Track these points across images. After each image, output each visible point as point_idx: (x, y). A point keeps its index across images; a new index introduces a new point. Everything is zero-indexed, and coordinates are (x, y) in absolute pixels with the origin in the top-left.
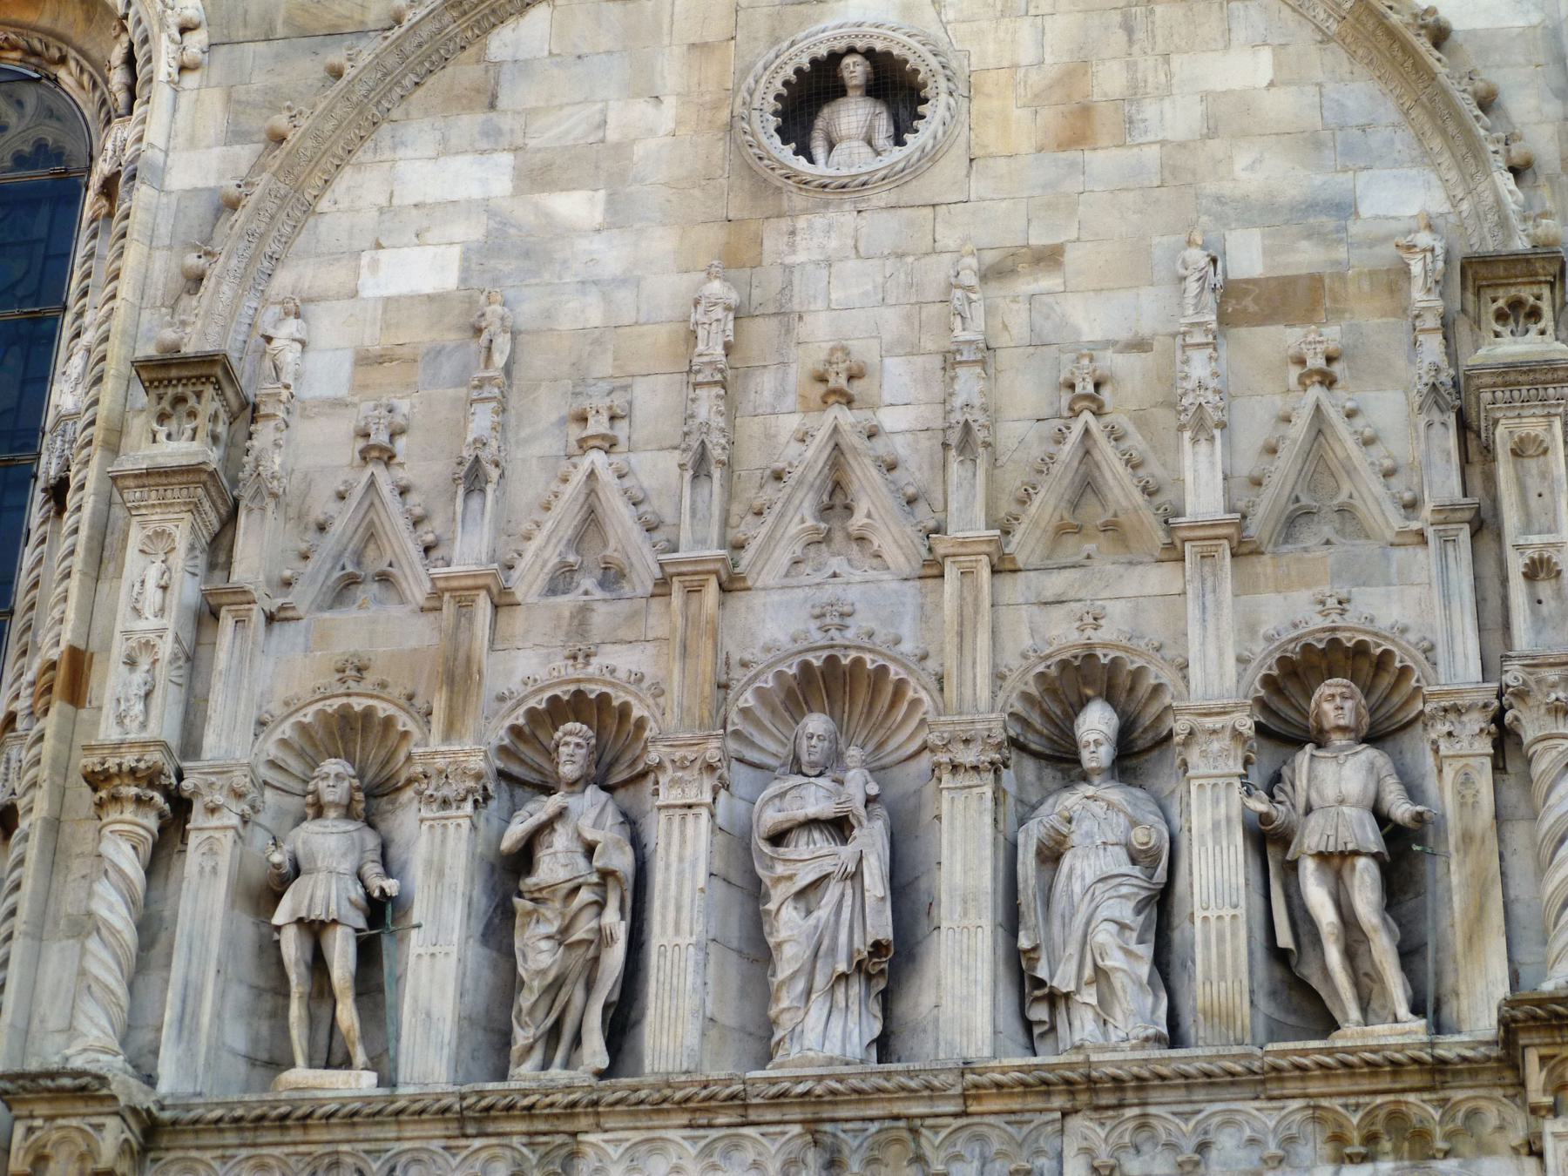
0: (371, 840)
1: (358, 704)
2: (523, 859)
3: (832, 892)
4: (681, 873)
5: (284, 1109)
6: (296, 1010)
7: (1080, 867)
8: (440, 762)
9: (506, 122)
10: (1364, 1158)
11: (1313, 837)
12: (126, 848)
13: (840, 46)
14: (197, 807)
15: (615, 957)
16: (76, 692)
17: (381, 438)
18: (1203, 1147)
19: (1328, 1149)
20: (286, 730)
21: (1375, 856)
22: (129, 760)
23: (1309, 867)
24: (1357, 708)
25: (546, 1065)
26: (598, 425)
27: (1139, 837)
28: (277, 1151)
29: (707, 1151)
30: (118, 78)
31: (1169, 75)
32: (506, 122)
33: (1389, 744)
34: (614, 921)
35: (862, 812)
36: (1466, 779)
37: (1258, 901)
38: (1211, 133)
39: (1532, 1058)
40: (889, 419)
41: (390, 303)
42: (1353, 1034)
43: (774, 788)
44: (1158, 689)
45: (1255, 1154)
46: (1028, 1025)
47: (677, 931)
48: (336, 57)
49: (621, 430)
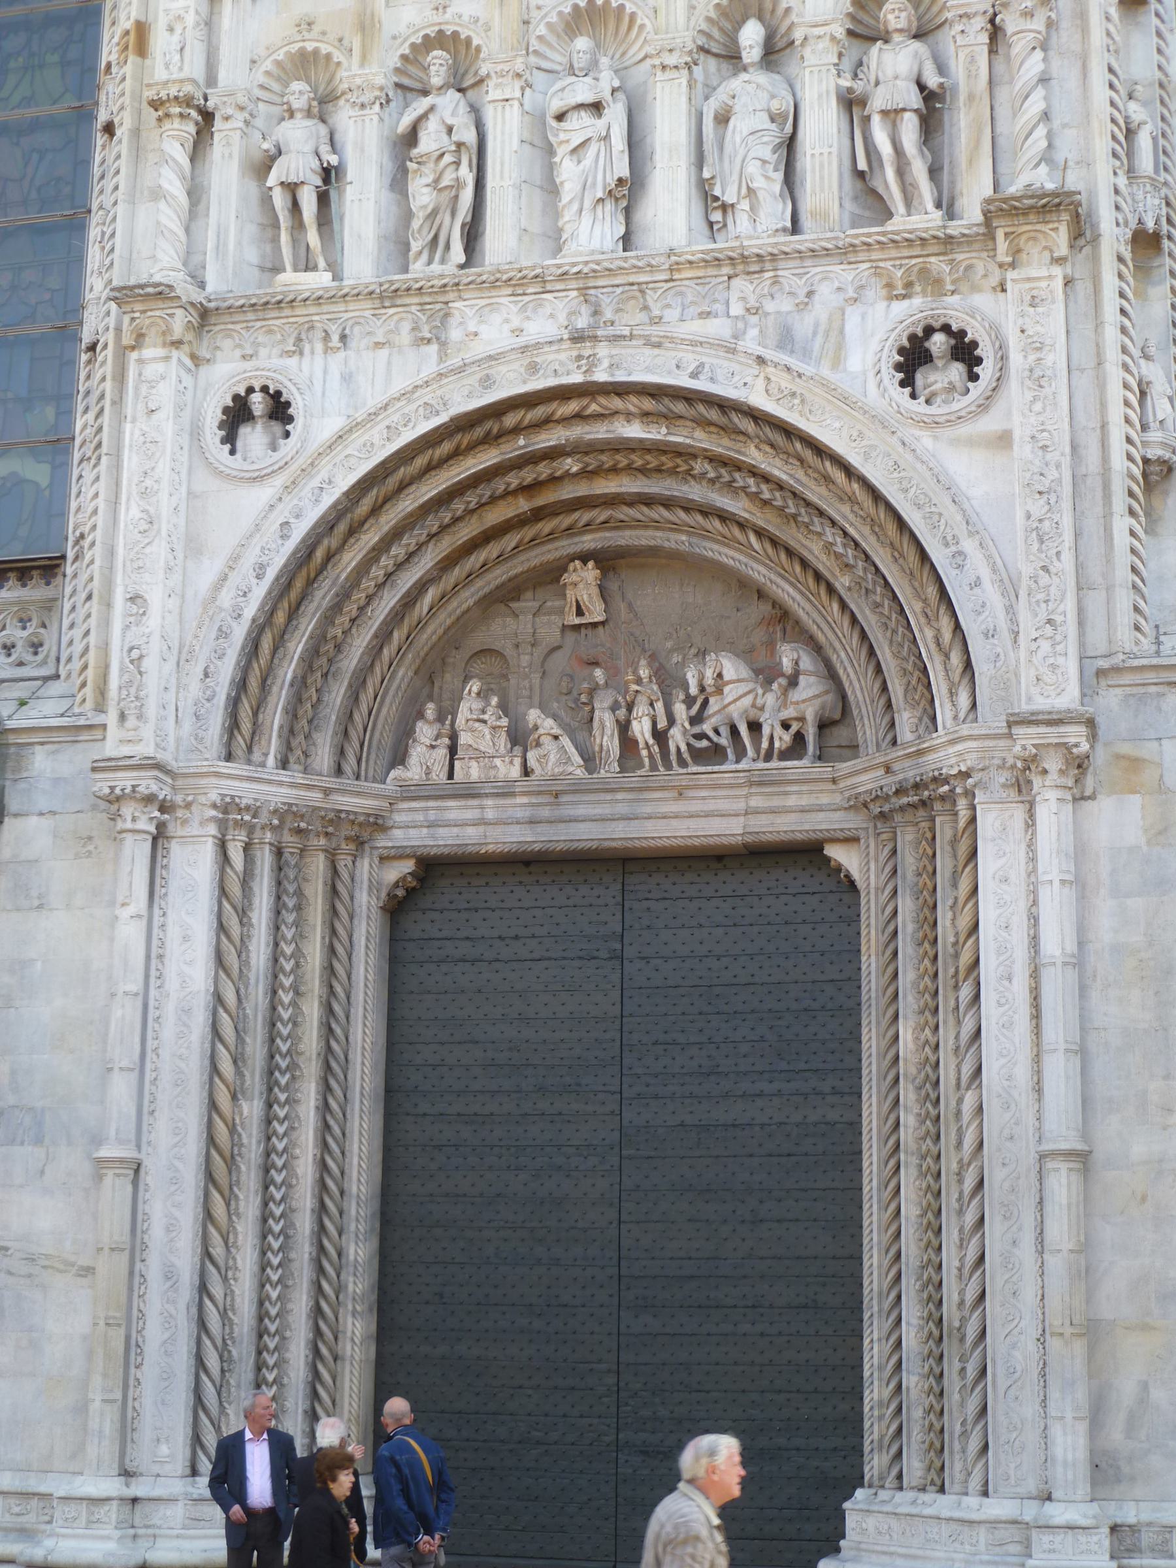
0: (323, 130)
1: (310, 46)
2: (411, 137)
4: (503, 142)
5: (279, 298)
6: (284, 237)
7: (740, 126)
8: (358, 81)
10: (904, 297)
11: (878, 101)
12: (177, 145)
14: (217, 117)
15: (467, 195)
16: (142, 49)
18: (810, 294)
19: (884, 292)
20: (268, 65)
21: (916, 111)
22: (173, 92)
23: (876, 120)
24: (909, 17)
25: (430, 262)
27: (775, 105)
28: (277, 322)
29: (524, 309)
33: (930, 38)
35: (608, 97)
36: (972, 60)
37: (847, 142)
39: (1000, 234)
42: (901, 222)
43: (559, 85)
44: (788, 10)
45: (841, 296)
47: (502, 178)
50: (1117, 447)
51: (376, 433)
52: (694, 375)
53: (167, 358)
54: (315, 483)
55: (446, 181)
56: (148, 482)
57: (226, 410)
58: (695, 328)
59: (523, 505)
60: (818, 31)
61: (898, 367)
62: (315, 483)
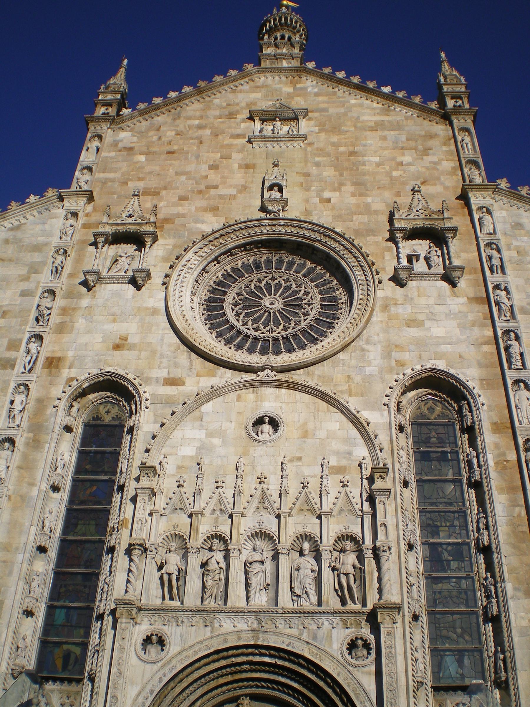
1: (177, 533)
3: (260, 574)
9: (204, 424)
13: (264, 415)
14: (148, 550)
17: (181, 483)
20: (164, 536)
22: (137, 542)
26: (220, 484)
28: (162, 615)
30: (133, 407)
31: (321, 426)
32: (204, 424)
34: (223, 577)
38: (328, 438)
40: (271, 487)
41: (183, 457)
46: (293, 600)
48: (175, 410)
49: (224, 485)
50: (410, 678)
51: (190, 652)
52: (287, 645)
53: (130, 623)
54: (170, 666)
55: (217, 577)
56: (121, 661)
57: (144, 640)
58: (288, 631)
59: (230, 678)
60: (326, 548)
61: (347, 649)
62: (170, 666)
